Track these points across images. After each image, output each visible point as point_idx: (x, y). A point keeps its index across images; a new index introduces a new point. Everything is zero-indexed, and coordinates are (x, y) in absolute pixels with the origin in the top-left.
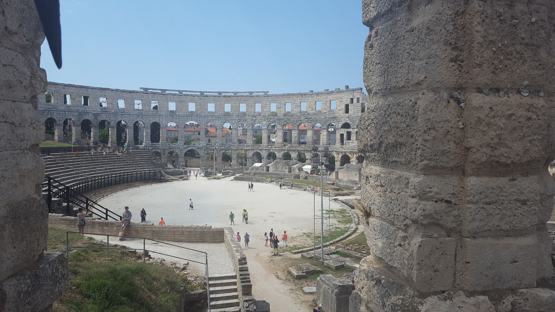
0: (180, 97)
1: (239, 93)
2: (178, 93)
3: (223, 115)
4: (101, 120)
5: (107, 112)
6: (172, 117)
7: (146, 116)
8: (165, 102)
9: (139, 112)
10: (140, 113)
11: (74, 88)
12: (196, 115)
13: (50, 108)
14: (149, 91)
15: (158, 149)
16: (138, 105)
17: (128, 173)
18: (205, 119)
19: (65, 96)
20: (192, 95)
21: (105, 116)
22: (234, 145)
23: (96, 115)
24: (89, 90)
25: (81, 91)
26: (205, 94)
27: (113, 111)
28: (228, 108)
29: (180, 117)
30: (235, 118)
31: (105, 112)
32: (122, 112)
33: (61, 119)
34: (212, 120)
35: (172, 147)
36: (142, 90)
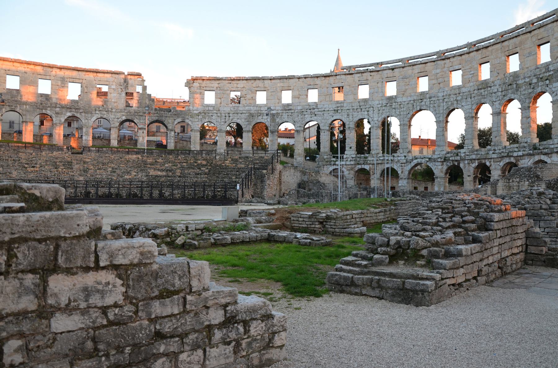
3: (476, 88)
5: (291, 110)
6: (389, 108)
7: (348, 111)
11: (245, 82)
12: (430, 98)
13: (209, 110)
18: (443, 103)
20: (423, 62)
22: (495, 150)
24: (266, 82)
25: (254, 85)
27: (299, 108)
28: (485, 73)
29: (402, 106)
31: (288, 110)
32: (314, 109)
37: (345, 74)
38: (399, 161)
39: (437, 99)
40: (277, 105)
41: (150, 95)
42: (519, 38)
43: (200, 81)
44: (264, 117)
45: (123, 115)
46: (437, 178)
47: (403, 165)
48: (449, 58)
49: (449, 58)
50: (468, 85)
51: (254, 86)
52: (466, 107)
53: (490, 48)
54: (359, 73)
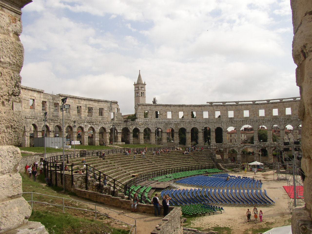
0: (237, 106)
1: (285, 99)
2: (235, 103)
4: (180, 128)
5: (184, 122)
6: (231, 123)
7: (212, 123)
8: (226, 112)
9: (207, 120)
10: (207, 121)
11: (162, 107)
14: (214, 104)
15: (221, 148)
16: (206, 115)
17: (192, 166)
18: (257, 123)
19: (157, 112)
20: (246, 104)
21: (183, 125)
23: (177, 124)
24: (172, 107)
26: (257, 102)
27: (188, 121)
28: (275, 112)
29: (237, 122)
30: (282, 121)
31: (183, 122)
33: (154, 128)
34: (263, 123)
35: (232, 146)
36: (209, 104)
37: (209, 106)
38: (237, 147)
39: (253, 121)
40: (177, 119)
41: (121, 114)
42: (291, 103)
43: (142, 106)
44: (172, 125)
45: (111, 125)
46: (255, 154)
47: (239, 148)
48: (259, 104)
49: (259, 104)
50: (268, 116)
51: (167, 109)
52: (268, 125)
53: (278, 104)
54: (216, 106)
